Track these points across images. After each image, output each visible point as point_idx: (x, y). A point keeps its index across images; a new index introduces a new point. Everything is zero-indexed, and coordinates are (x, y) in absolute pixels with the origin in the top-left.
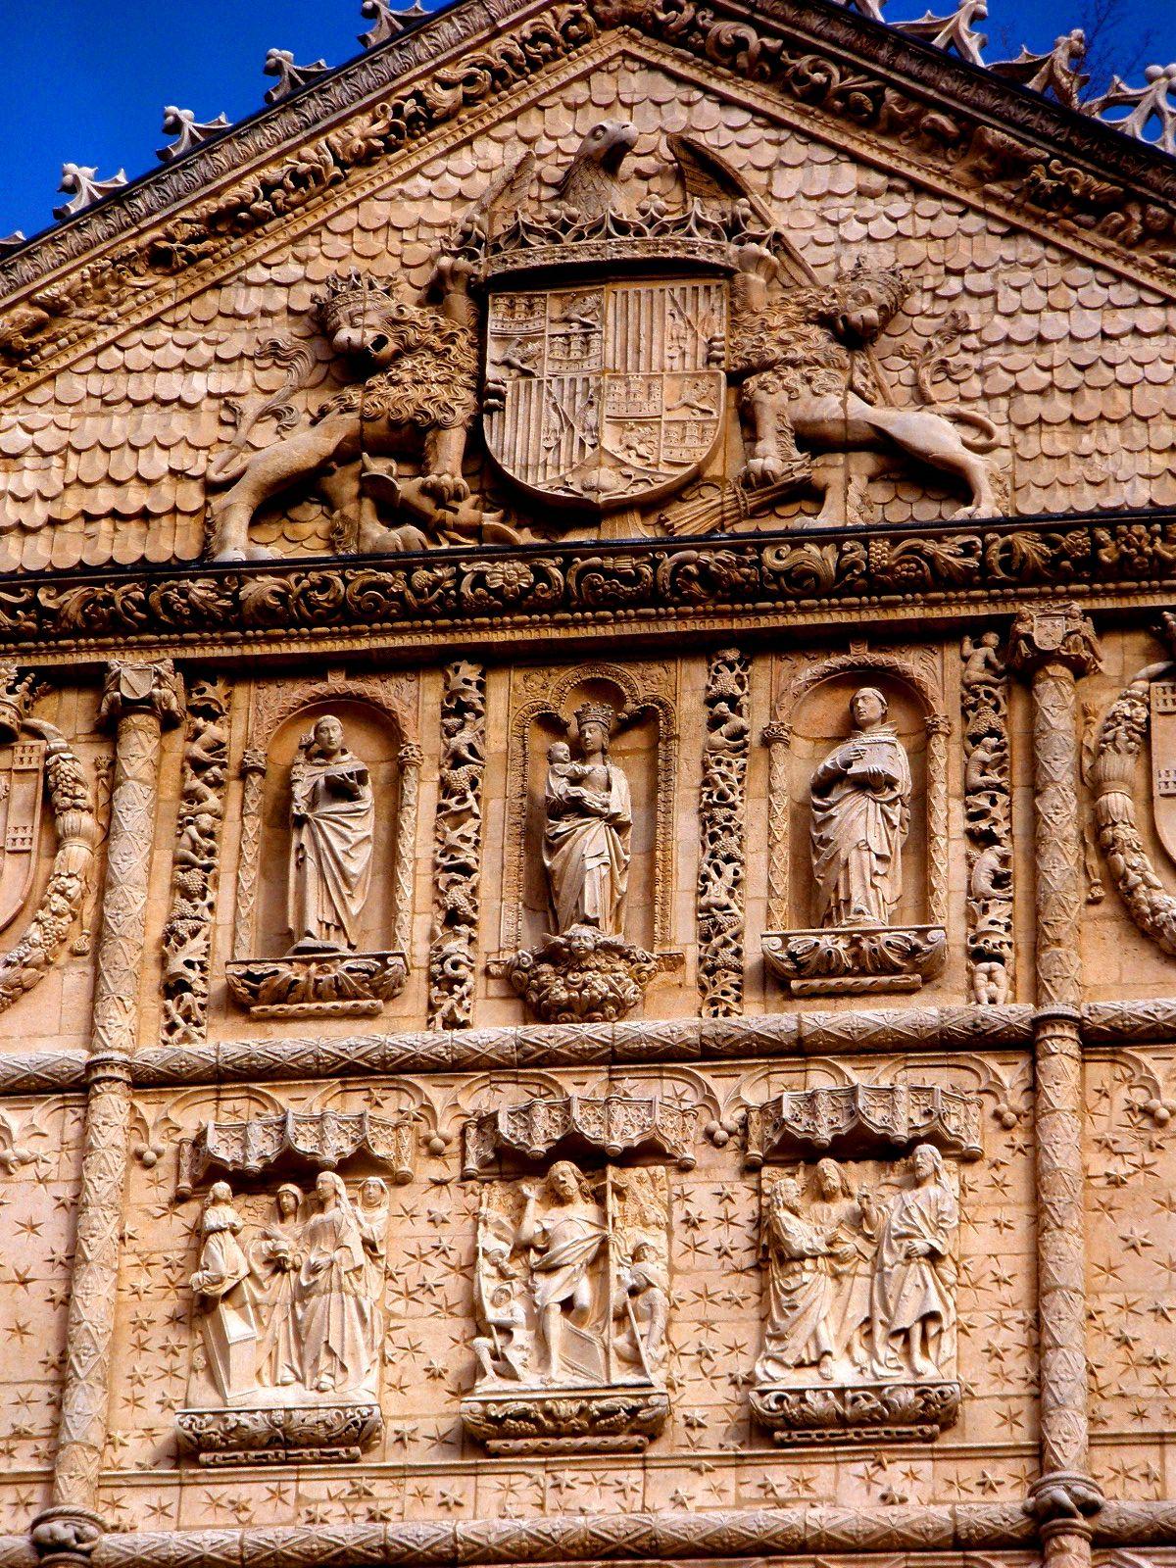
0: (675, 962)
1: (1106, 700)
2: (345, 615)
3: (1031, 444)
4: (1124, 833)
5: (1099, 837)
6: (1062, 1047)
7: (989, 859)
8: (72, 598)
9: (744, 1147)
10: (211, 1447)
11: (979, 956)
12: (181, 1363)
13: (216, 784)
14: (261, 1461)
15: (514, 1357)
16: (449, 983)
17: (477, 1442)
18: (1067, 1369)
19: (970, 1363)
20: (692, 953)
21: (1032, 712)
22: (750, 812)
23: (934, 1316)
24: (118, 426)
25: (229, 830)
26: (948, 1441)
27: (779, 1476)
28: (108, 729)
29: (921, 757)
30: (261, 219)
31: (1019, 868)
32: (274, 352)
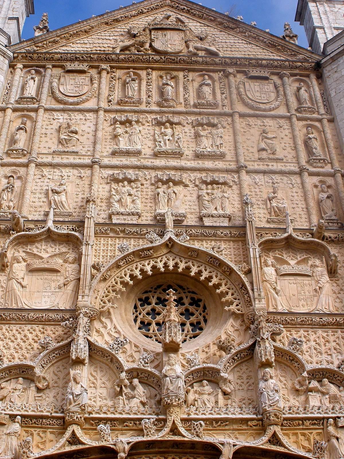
0: (181, 103)
1: (238, 80)
2: (133, 61)
3: (225, 52)
4: (243, 93)
5: (239, 94)
6: (237, 116)
7: (224, 95)
8: (96, 56)
9: (192, 125)
10: (117, 153)
11: (224, 106)
12: (112, 144)
13: (115, 80)
14: (124, 155)
15: (162, 145)
16: (149, 103)
17: (156, 155)
18: (241, 151)
19: (227, 149)
20: (183, 103)
21: (229, 80)
22: (190, 88)
23: (222, 144)
24: (100, 41)
25: (117, 85)
26: (224, 159)
27: (200, 162)
28: (99, 73)
29: (214, 84)
30: (120, 21)
31: (228, 97)
32: (122, 35)
